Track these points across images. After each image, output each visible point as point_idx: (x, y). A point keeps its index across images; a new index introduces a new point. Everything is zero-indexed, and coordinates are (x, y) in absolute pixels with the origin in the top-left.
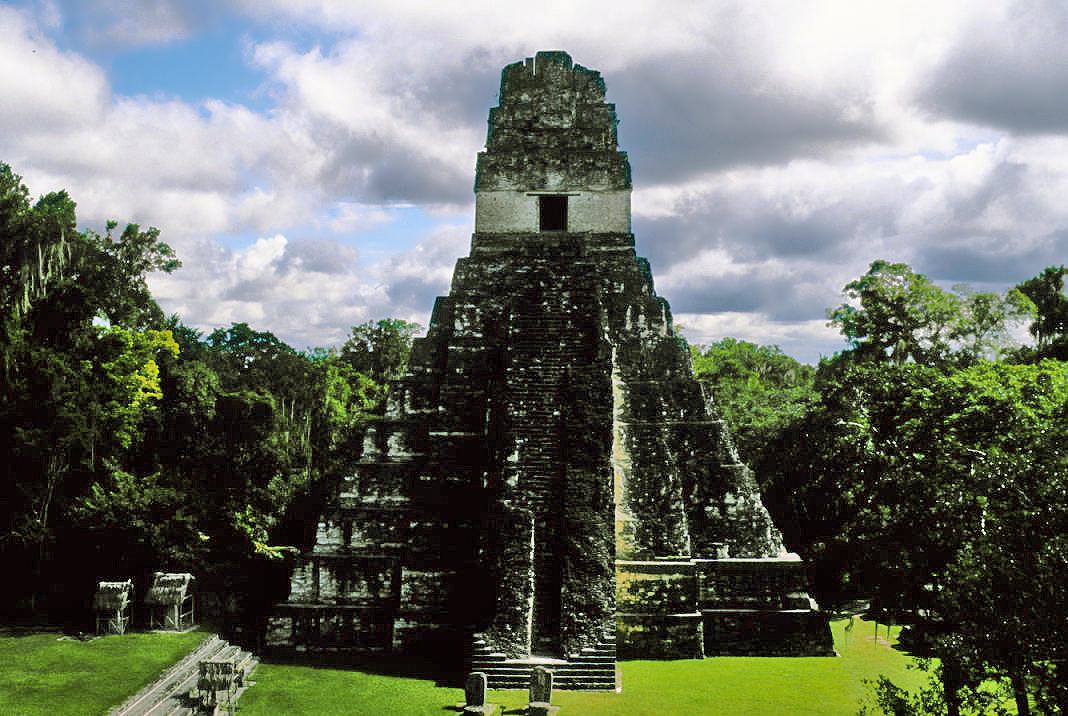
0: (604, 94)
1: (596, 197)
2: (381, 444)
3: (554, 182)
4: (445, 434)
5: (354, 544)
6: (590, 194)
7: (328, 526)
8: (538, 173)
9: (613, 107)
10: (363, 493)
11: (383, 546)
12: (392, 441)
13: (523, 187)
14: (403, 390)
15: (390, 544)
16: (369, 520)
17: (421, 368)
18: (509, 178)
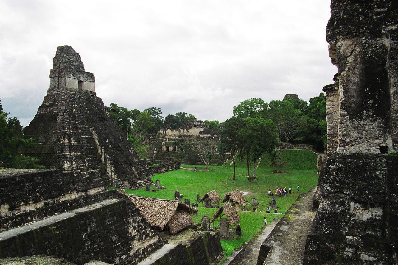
0: (80, 59)
1: (89, 83)
2: (70, 141)
3: (82, 78)
4: (85, 137)
5: (74, 166)
6: (88, 82)
7: (67, 162)
8: (78, 75)
9: (83, 62)
10: (70, 153)
11: (80, 165)
12: (72, 139)
13: (76, 78)
14: (69, 126)
15: (82, 165)
16: (76, 159)
17: (69, 121)
18: (73, 75)
